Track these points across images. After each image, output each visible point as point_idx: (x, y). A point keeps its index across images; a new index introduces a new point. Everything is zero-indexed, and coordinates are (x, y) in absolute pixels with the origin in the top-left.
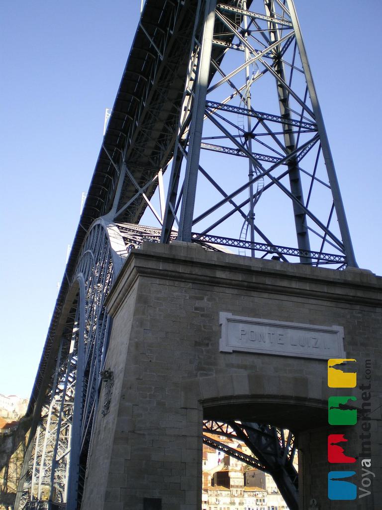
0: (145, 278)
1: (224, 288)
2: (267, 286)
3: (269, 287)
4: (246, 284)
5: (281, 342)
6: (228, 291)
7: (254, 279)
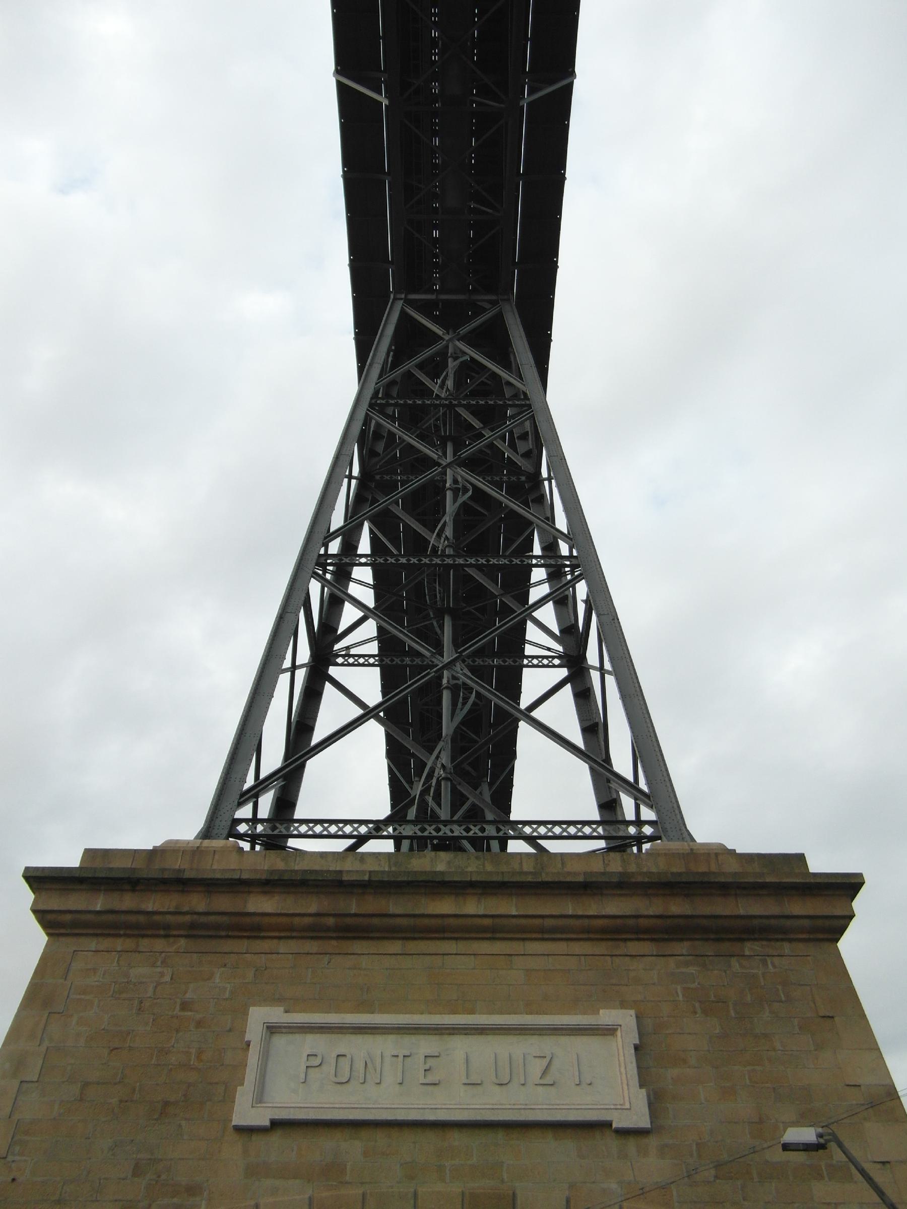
0: (63, 939)
1: (275, 941)
2: (392, 921)
3: (398, 921)
4: (331, 921)
5: (430, 1079)
6: (284, 947)
7: (354, 906)
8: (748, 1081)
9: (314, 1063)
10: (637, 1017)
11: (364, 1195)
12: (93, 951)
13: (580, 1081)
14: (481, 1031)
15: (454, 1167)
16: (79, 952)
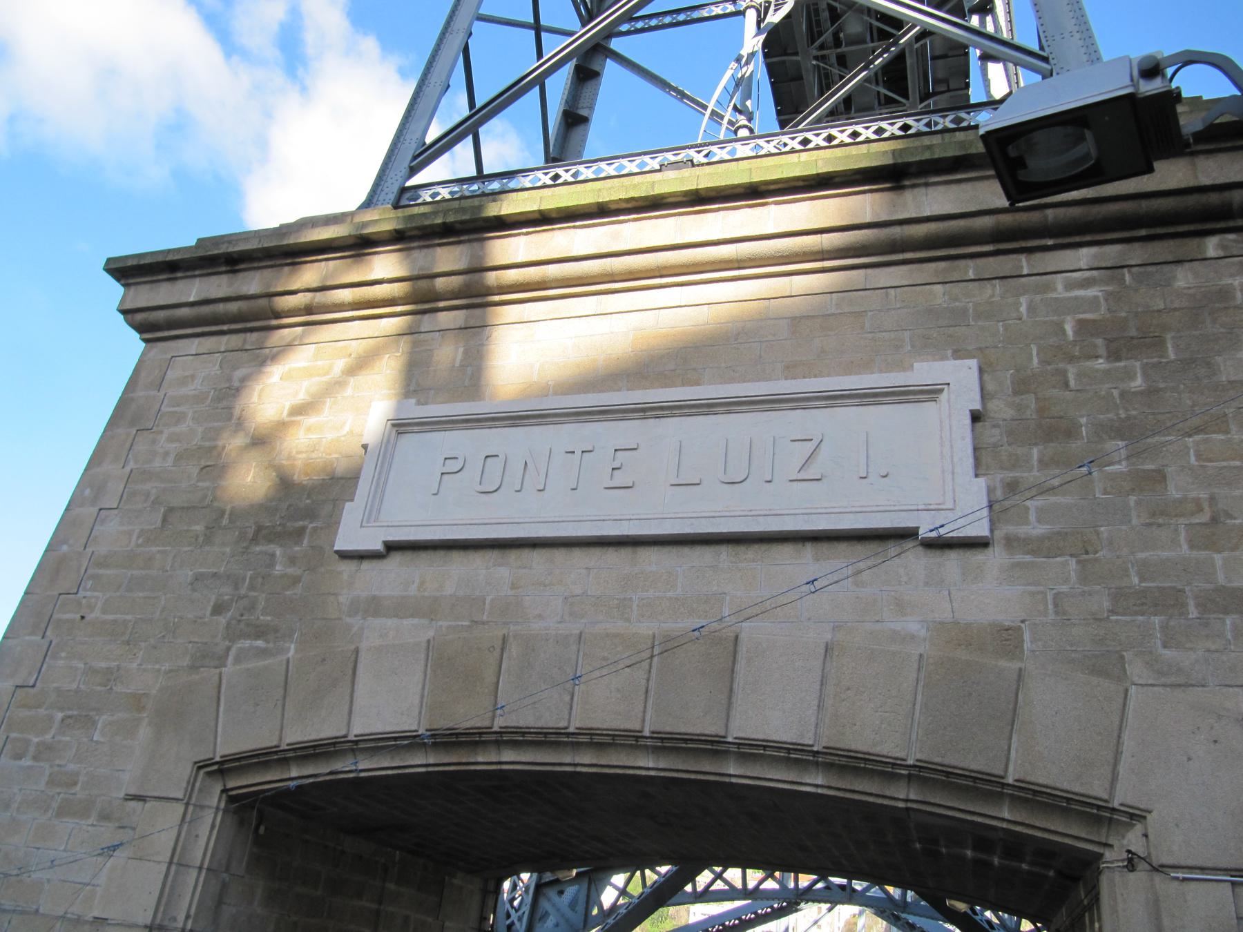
5: (619, 479)
8: (1193, 460)
9: (452, 468)
10: (981, 371)
11: (504, 639)
12: (192, 355)
13: (867, 472)
14: (708, 408)
15: (644, 601)
16: (177, 358)
